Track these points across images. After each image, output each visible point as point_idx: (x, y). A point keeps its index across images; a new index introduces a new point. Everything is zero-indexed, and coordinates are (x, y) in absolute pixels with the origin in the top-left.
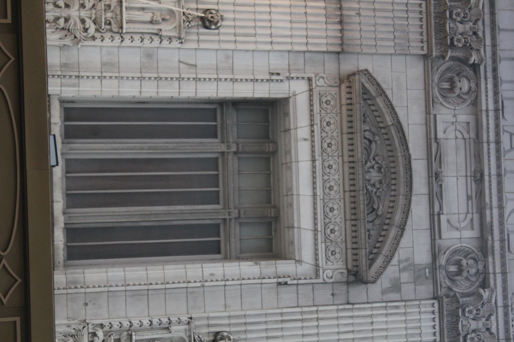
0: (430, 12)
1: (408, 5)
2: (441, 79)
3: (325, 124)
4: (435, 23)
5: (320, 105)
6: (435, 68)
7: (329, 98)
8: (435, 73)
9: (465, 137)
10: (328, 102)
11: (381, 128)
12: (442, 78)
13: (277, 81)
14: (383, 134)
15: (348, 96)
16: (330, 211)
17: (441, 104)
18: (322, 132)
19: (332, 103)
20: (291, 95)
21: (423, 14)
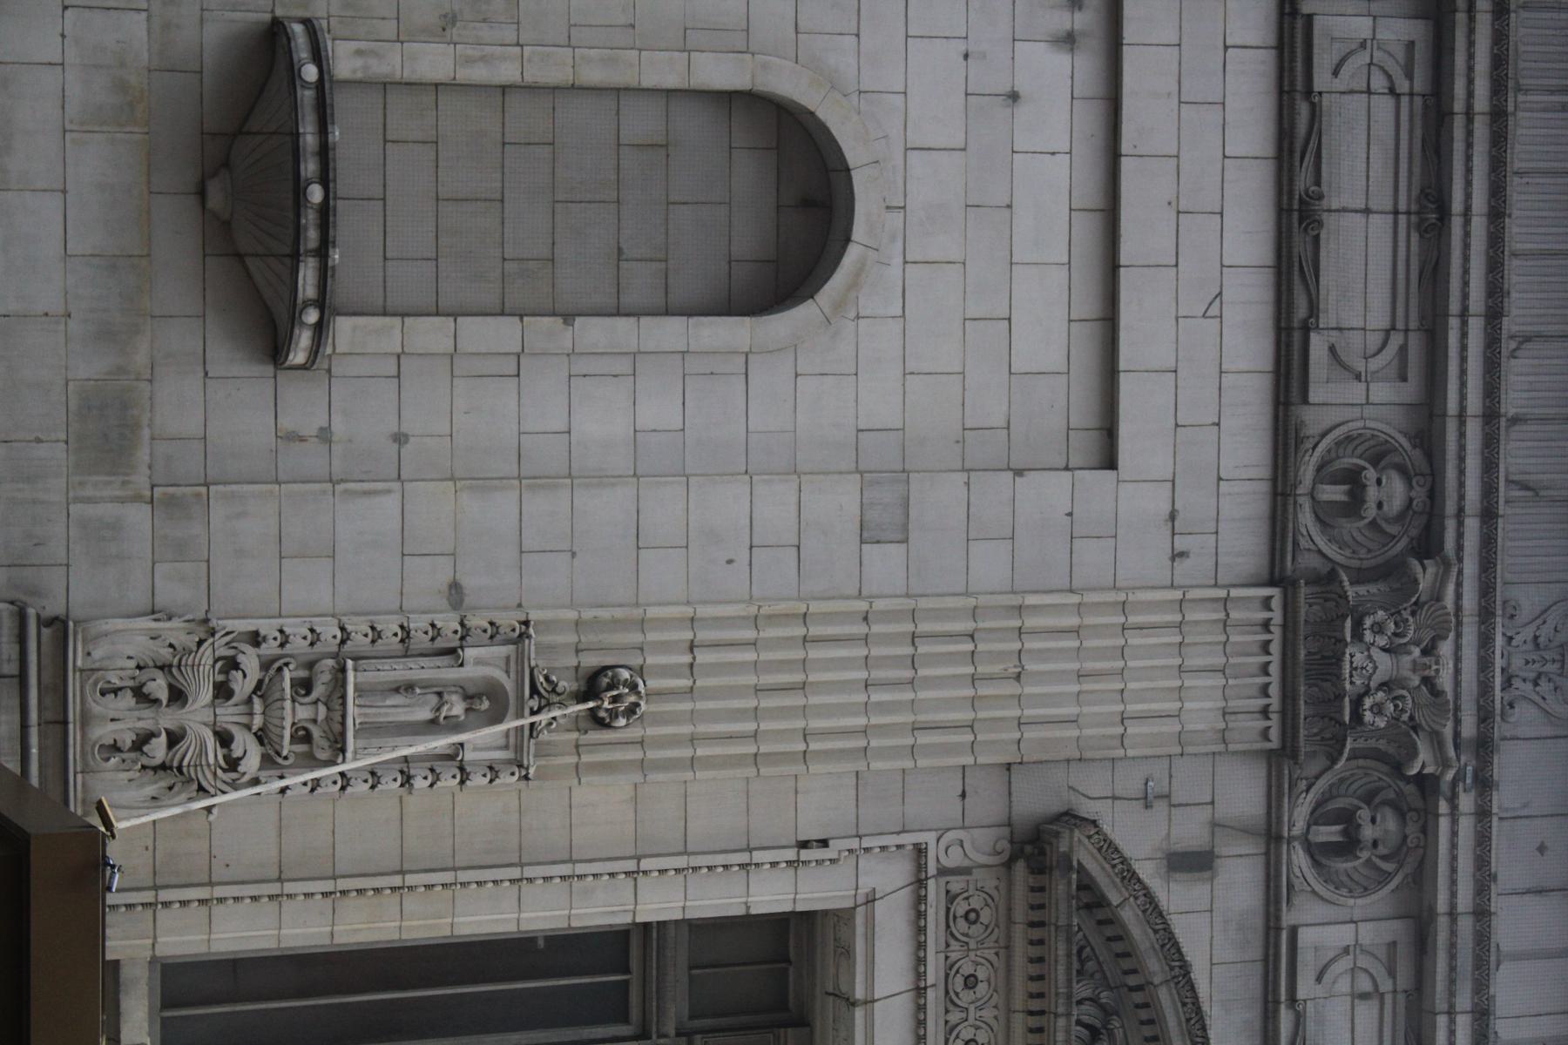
0: (1295, 623)
1: (1229, 605)
2: (1318, 816)
3: (959, 982)
4: (1309, 653)
5: (948, 926)
6: (1303, 785)
7: (976, 903)
8: (1301, 800)
9: (1382, 989)
10: (972, 916)
11: (1131, 989)
12: (1320, 811)
13: (819, 862)
14: (1137, 1006)
15: (1034, 970)
16: (966, 986)
17: (1314, 892)
18: (951, 1008)
19: (986, 916)
20: (861, 900)
21: (1272, 628)
